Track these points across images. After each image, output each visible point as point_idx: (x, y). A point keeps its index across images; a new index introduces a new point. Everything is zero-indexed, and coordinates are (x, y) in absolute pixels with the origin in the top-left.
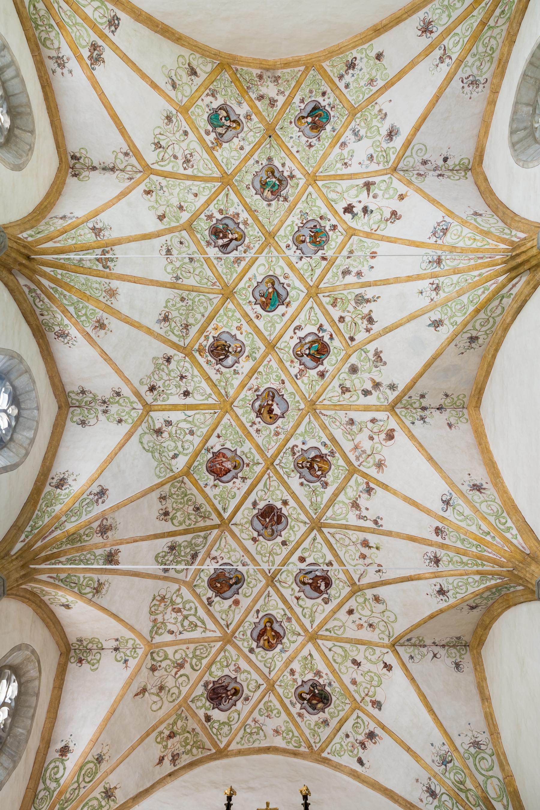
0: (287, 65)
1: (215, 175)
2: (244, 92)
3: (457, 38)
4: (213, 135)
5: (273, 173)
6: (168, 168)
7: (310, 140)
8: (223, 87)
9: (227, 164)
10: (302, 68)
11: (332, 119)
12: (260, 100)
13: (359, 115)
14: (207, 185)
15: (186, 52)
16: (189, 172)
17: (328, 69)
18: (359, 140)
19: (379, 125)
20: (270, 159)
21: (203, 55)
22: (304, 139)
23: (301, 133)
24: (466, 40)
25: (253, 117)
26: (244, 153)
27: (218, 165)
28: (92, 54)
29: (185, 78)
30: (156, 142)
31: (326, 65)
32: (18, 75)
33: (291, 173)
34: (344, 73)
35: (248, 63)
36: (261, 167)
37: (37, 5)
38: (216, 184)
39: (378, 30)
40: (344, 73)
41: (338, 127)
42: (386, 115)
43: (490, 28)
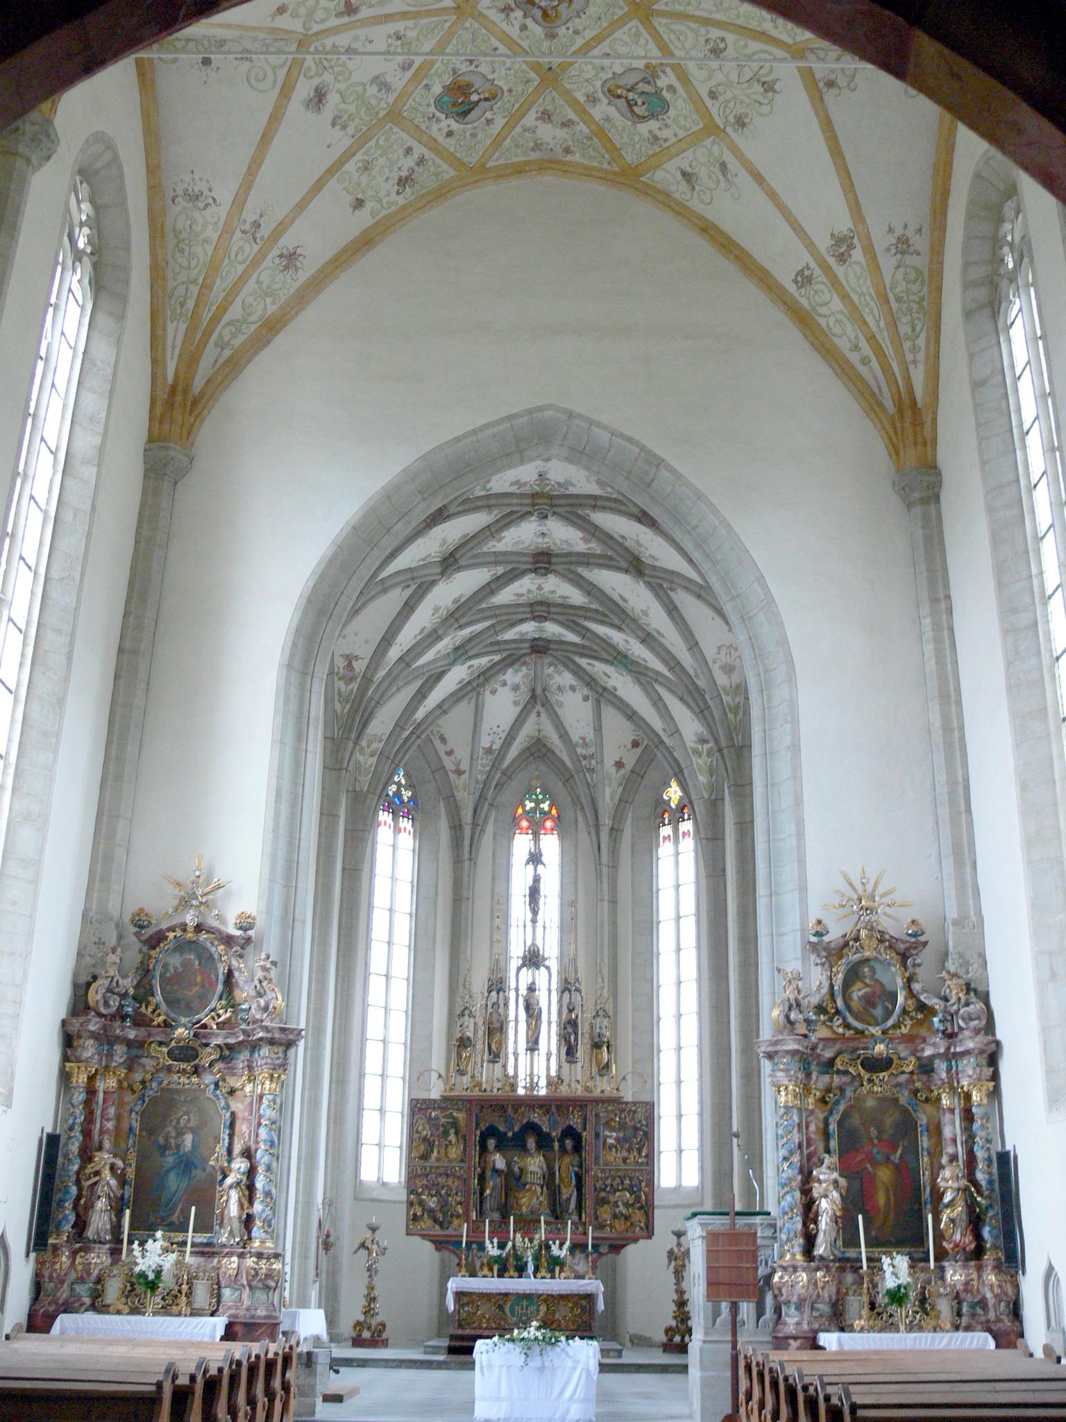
0: (519, 170)
1: (664, 21)
2: (600, 132)
3: (240, 258)
4: (662, 82)
5: (545, 14)
6: (754, 46)
7: (472, 68)
8: (637, 146)
9: (638, 35)
10: (490, 164)
11: (432, 101)
12: (570, 121)
13: (382, 114)
14: (682, 8)
15: (695, 204)
16: (715, 33)
17: (444, 166)
18: (377, 77)
19: (343, 106)
20: (551, 36)
21: (668, 195)
22: (484, 69)
23: (490, 77)
24: (227, 261)
25: (582, 99)
26: (604, 47)
27: (657, 37)
28: (848, 251)
29: (703, 172)
30: (770, 94)
31: (449, 172)
32: (966, 266)
33: (508, 15)
34: (416, 169)
35: (587, 173)
36: (569, 24)
37: (909, 330)
38: (663, 7)
39: (364, 243)
40: (416, 169)
41: (420, 90)
42: (333, 125)
43: (195, 281)
